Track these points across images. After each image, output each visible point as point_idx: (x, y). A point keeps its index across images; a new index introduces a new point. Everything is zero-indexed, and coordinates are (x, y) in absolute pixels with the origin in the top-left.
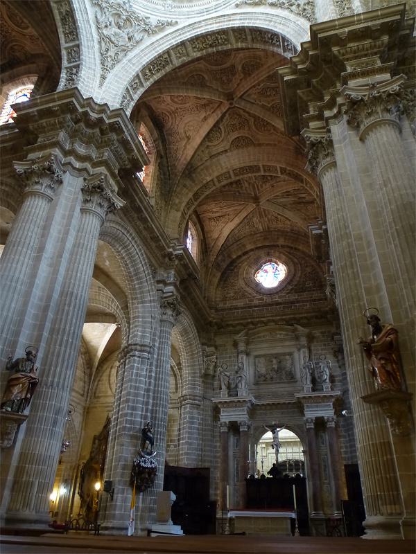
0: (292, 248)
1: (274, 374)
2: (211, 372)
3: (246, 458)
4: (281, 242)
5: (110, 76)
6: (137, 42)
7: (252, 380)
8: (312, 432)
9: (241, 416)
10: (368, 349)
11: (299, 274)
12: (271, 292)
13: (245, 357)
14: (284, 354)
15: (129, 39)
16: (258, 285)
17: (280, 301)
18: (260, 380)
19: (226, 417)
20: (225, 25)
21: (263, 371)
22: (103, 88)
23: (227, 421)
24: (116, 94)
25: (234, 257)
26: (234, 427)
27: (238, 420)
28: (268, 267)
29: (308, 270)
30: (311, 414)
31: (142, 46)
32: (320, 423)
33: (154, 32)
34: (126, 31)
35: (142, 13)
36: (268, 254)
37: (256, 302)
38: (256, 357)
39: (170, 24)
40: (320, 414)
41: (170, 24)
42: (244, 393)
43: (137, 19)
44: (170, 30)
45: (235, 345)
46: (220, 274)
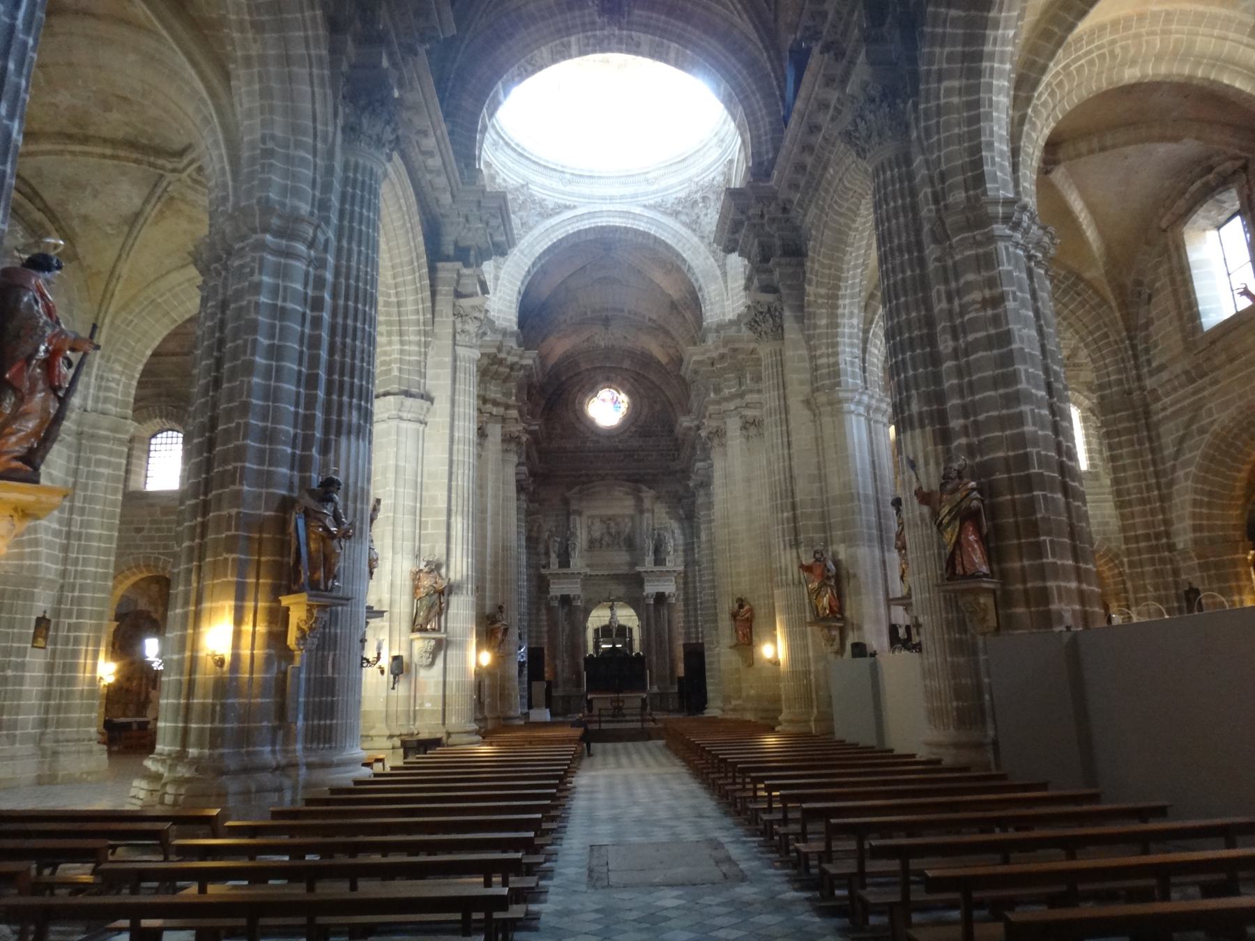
0: (638, 374)
1: (607, 538)
2: (534, 534)
3: (577, 630)
4: (626, 364)
5: (502, 274)
6: (531, 228)
7: (585, 545)
8: (652, 608)
9: (573, 588)
10: (734, 616)
11: (645, 410)
12: (610, 434)
13: (577, 518)
14: (623, 516)
15: (523, 224)
16: (592, 422)
17: (620, 446)
18: (592, 544)
19: (557, 589)
20: (629, 223)
21: (597, 535)
22: (498, 294)
23: (558, 595)
24: (510, 302)
25: (564, 379)
26: (566, 600)
27: (572, 595)
28: (606, 394)
29: (658, 407)
30: (650, 589)
31: (536, 232)
32: (660, 598)
33: (550, 216)
34: (520, 214)
35: (540, 195)
36: (608, 379)
37: (589, 444)
38: (589, 517)
39: (567, 207)
40: (661, 589)
41: (567, 207)
42: (578, 562)
43: (534, 202)
44: (567, 215)
45: (566, 502)
46: (543, 402)
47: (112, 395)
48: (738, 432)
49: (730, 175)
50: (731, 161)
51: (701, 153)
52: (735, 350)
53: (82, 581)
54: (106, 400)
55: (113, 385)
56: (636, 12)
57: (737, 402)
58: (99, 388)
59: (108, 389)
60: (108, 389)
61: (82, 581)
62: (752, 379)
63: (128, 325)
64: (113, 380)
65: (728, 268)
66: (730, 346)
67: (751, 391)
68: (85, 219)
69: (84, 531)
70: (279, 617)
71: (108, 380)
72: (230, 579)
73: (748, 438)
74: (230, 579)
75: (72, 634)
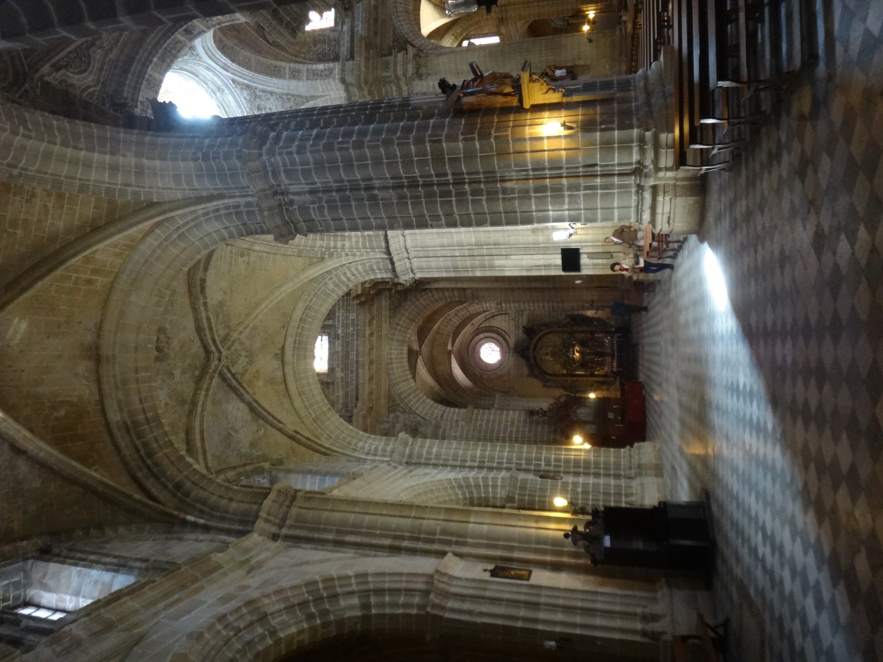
47: (380, 448)
48: (424, 83)
49: (243, 84)
50: (234, 81)
51: (226, 108)
52: (366, 82)
53: (514, 459)
54: (384, 450)
55: (373, 447)
56: (125, 94)
57: (402, 83)
58: (375, 455)
59: (376, 450)
60: (376, 450)
61: (514, 459)
62: (387, 72)
63: (331, 437)
64: (370, 447)
65: (308, 95)
66: (363, 85)
67: (395, 71)
68: (252, 445)
69: (478, 460)
70: (539, 108)
71: (370, 450)
72: (509, 133)
73: (428, 74)
74: (509, 133)
75: (553, 463)
